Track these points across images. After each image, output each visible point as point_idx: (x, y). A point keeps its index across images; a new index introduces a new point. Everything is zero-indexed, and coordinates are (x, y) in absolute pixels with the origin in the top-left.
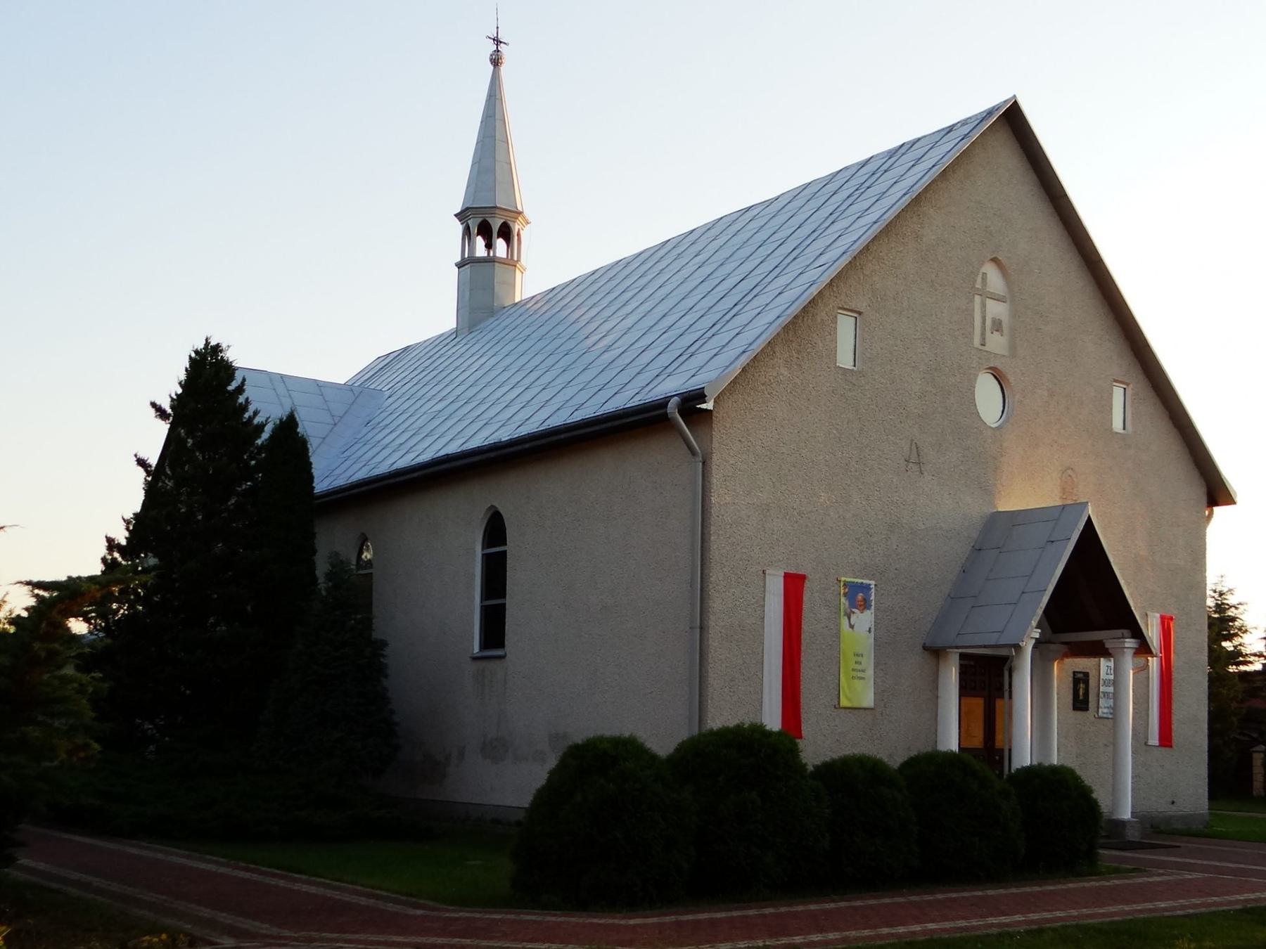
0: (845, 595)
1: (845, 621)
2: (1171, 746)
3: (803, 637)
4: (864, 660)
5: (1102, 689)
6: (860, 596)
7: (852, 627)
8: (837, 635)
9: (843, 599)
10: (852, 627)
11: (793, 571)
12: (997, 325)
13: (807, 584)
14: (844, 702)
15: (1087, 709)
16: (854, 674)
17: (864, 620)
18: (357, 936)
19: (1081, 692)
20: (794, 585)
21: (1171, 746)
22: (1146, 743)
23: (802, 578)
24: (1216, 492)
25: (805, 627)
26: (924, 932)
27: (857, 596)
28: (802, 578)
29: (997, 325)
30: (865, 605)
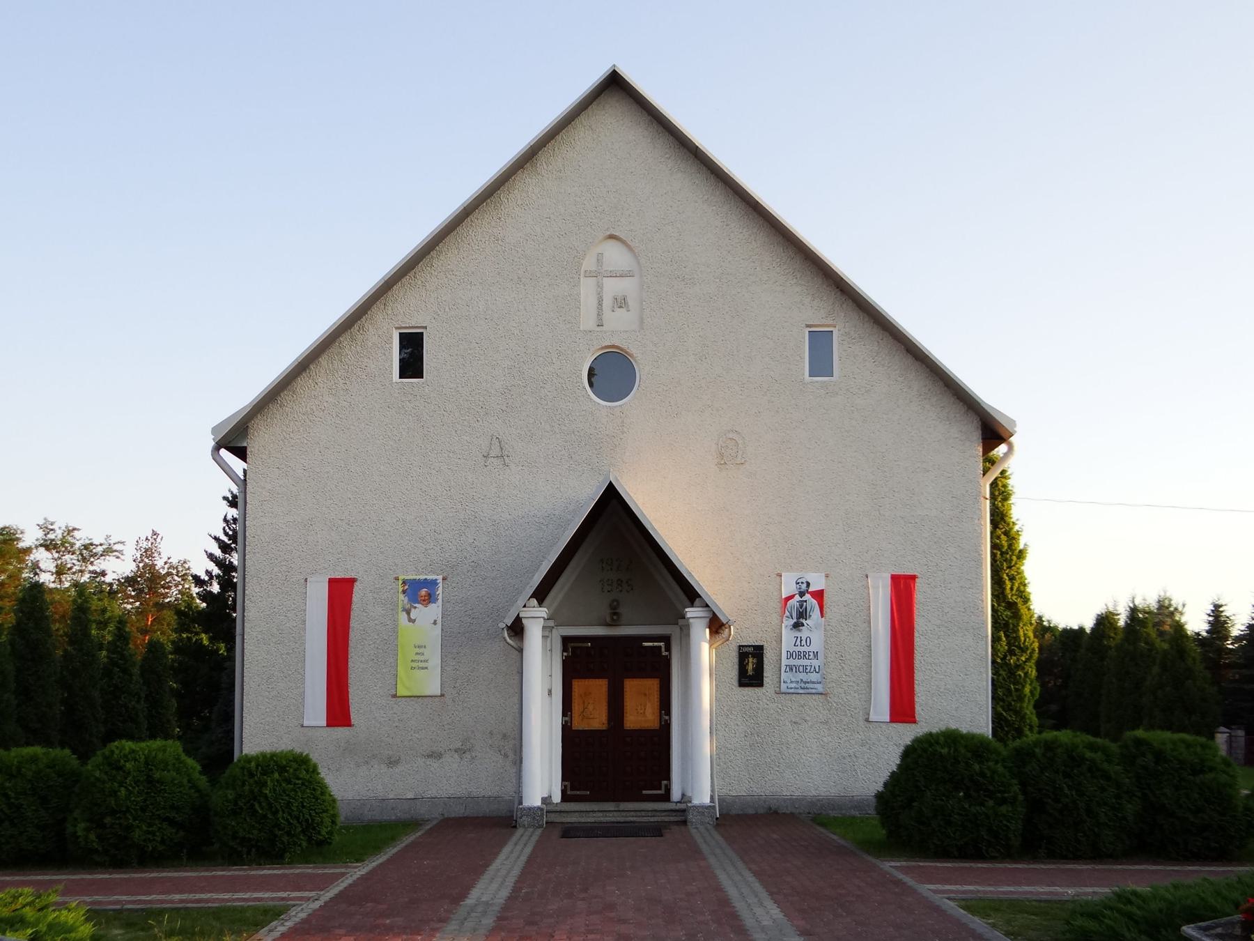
0: (404, 592)
1: (403, 617)
2: (915, 722)
3: (352, 635)
4: (426, 651)
5: (784, 662)
6: (423, 592)
7: (410, 620)
8: (395, 630)
9: (401, 596)
10: (411, 621)
11: (339, 575)
12: (621, 302)
13: (357, 588)
14: (402, 691)
15: (761, 685)
16: (414, 665)
17: (428, 614)
18: (139, 898)
19: (750, 667)
20: (341, 591)
21: (915, 722)
22: (867, 720)
23: (351, 582)
24: (993, 433)
25: (354, 624)
26: (1020, 884)
27: (421, 592)
28: (351, 582)
29: (621, 302)
30: (430, 599)
